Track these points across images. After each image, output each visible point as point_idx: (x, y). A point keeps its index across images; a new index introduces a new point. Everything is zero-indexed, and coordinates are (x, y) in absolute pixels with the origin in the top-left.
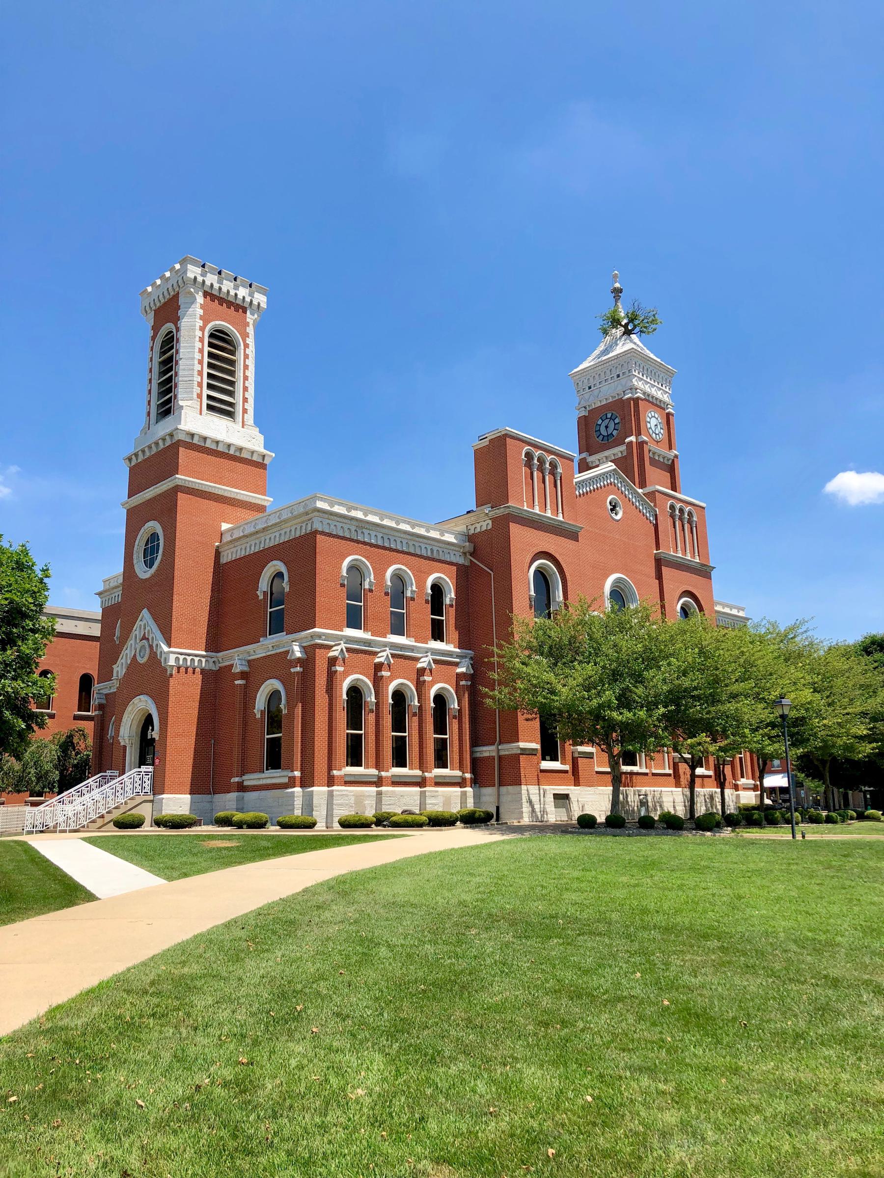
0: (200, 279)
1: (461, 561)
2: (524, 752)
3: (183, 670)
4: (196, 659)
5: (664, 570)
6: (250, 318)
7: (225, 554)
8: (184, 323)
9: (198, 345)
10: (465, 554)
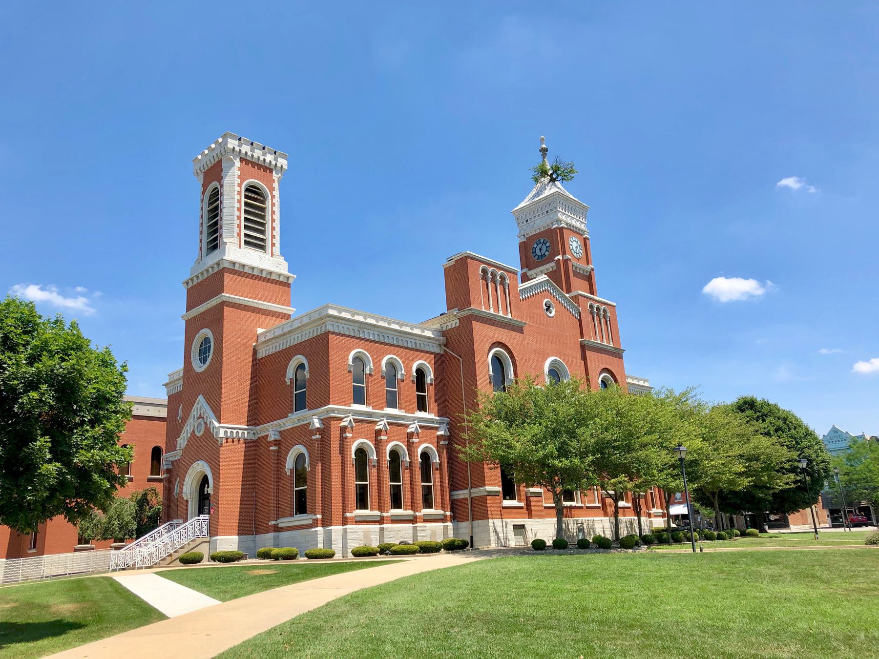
0: (237, 149)
1: (437, 350)
2: (490, 494)
3: (230, 440)
4: (240, 432)
5: (587, 352)
6: (275, 176)
7: (260, 351)
8: (226, 181)
9: (237, 197)
10: (440, 345)
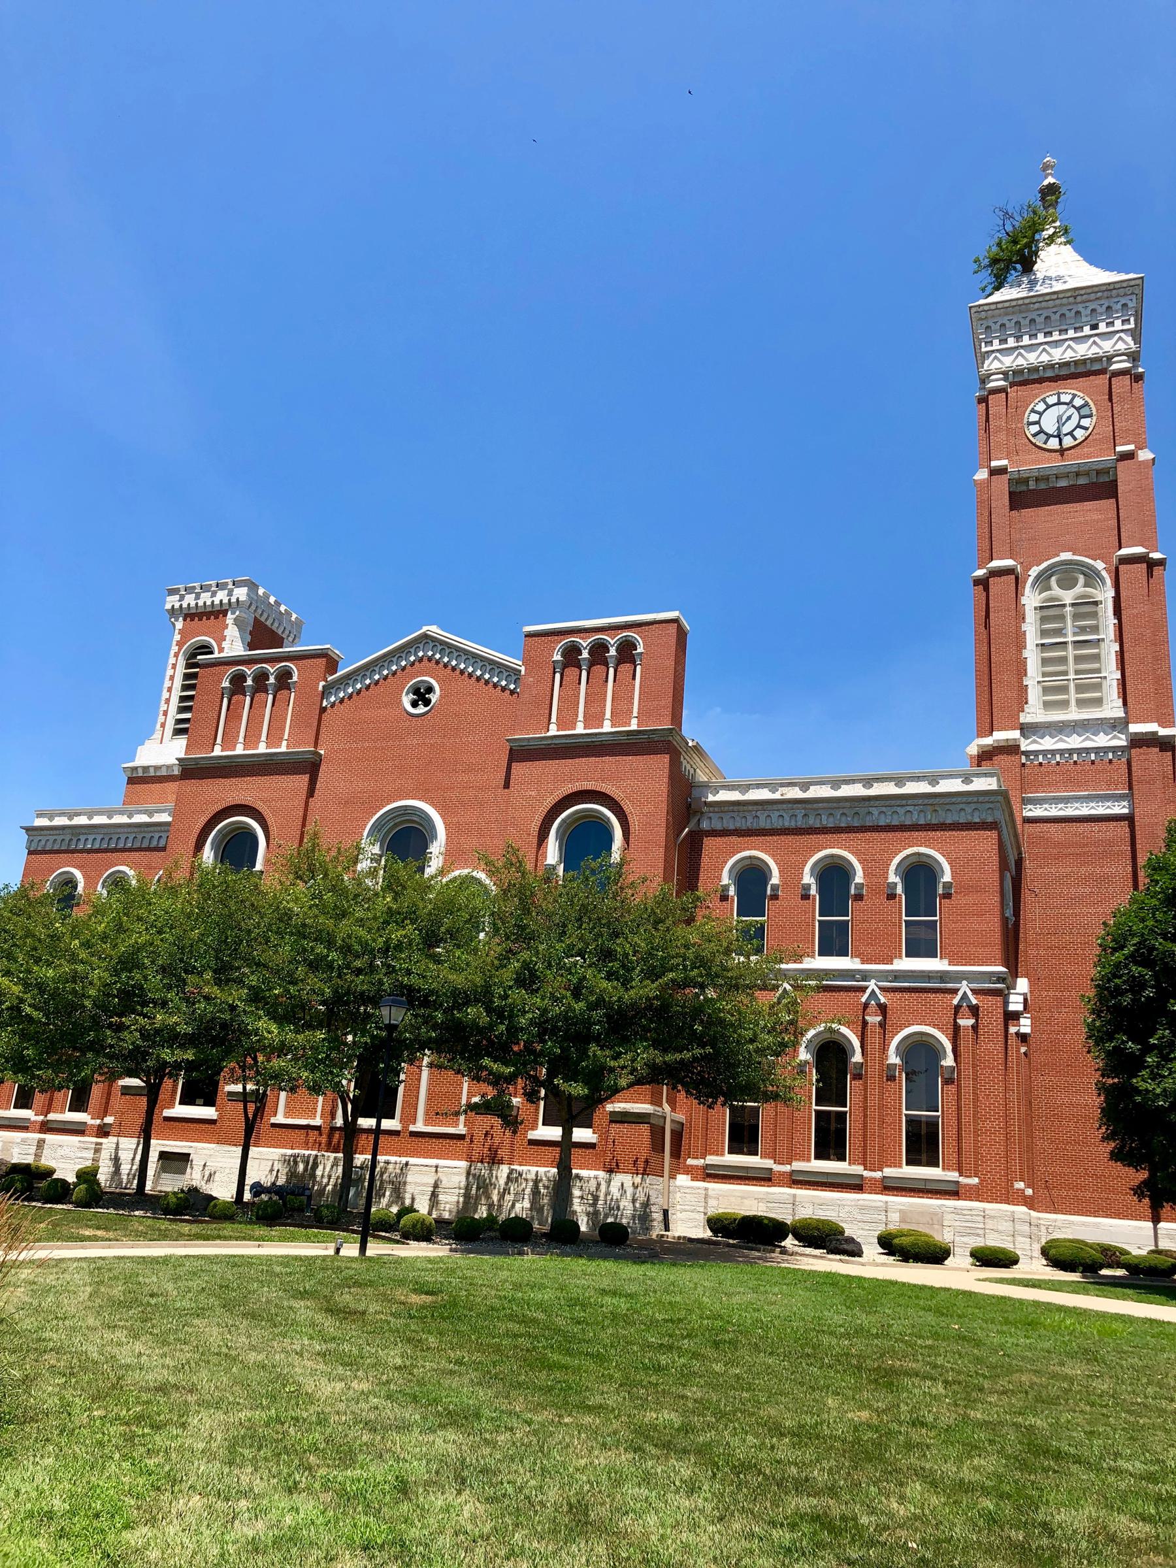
0: (177, 606)
6: (230, 618)
